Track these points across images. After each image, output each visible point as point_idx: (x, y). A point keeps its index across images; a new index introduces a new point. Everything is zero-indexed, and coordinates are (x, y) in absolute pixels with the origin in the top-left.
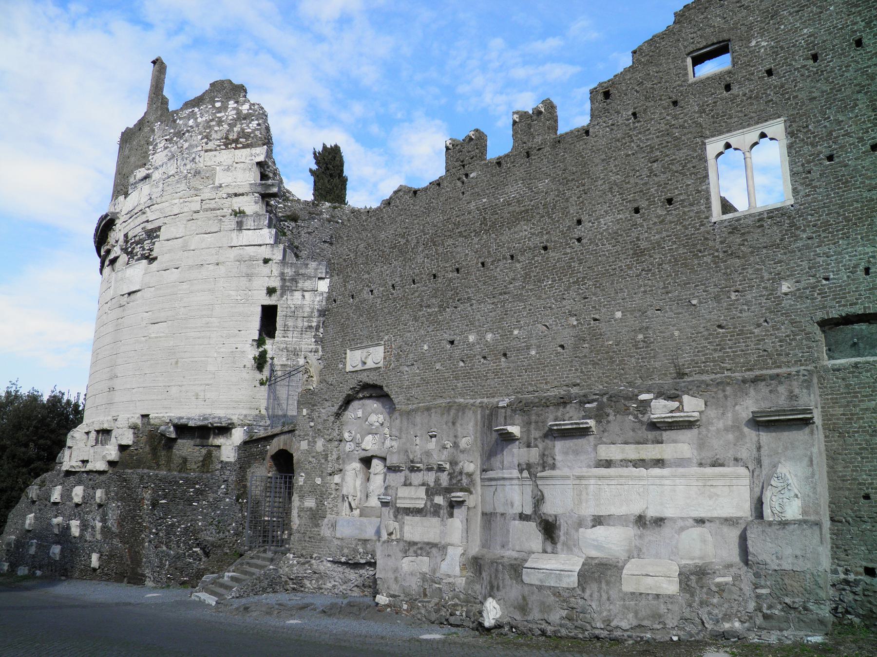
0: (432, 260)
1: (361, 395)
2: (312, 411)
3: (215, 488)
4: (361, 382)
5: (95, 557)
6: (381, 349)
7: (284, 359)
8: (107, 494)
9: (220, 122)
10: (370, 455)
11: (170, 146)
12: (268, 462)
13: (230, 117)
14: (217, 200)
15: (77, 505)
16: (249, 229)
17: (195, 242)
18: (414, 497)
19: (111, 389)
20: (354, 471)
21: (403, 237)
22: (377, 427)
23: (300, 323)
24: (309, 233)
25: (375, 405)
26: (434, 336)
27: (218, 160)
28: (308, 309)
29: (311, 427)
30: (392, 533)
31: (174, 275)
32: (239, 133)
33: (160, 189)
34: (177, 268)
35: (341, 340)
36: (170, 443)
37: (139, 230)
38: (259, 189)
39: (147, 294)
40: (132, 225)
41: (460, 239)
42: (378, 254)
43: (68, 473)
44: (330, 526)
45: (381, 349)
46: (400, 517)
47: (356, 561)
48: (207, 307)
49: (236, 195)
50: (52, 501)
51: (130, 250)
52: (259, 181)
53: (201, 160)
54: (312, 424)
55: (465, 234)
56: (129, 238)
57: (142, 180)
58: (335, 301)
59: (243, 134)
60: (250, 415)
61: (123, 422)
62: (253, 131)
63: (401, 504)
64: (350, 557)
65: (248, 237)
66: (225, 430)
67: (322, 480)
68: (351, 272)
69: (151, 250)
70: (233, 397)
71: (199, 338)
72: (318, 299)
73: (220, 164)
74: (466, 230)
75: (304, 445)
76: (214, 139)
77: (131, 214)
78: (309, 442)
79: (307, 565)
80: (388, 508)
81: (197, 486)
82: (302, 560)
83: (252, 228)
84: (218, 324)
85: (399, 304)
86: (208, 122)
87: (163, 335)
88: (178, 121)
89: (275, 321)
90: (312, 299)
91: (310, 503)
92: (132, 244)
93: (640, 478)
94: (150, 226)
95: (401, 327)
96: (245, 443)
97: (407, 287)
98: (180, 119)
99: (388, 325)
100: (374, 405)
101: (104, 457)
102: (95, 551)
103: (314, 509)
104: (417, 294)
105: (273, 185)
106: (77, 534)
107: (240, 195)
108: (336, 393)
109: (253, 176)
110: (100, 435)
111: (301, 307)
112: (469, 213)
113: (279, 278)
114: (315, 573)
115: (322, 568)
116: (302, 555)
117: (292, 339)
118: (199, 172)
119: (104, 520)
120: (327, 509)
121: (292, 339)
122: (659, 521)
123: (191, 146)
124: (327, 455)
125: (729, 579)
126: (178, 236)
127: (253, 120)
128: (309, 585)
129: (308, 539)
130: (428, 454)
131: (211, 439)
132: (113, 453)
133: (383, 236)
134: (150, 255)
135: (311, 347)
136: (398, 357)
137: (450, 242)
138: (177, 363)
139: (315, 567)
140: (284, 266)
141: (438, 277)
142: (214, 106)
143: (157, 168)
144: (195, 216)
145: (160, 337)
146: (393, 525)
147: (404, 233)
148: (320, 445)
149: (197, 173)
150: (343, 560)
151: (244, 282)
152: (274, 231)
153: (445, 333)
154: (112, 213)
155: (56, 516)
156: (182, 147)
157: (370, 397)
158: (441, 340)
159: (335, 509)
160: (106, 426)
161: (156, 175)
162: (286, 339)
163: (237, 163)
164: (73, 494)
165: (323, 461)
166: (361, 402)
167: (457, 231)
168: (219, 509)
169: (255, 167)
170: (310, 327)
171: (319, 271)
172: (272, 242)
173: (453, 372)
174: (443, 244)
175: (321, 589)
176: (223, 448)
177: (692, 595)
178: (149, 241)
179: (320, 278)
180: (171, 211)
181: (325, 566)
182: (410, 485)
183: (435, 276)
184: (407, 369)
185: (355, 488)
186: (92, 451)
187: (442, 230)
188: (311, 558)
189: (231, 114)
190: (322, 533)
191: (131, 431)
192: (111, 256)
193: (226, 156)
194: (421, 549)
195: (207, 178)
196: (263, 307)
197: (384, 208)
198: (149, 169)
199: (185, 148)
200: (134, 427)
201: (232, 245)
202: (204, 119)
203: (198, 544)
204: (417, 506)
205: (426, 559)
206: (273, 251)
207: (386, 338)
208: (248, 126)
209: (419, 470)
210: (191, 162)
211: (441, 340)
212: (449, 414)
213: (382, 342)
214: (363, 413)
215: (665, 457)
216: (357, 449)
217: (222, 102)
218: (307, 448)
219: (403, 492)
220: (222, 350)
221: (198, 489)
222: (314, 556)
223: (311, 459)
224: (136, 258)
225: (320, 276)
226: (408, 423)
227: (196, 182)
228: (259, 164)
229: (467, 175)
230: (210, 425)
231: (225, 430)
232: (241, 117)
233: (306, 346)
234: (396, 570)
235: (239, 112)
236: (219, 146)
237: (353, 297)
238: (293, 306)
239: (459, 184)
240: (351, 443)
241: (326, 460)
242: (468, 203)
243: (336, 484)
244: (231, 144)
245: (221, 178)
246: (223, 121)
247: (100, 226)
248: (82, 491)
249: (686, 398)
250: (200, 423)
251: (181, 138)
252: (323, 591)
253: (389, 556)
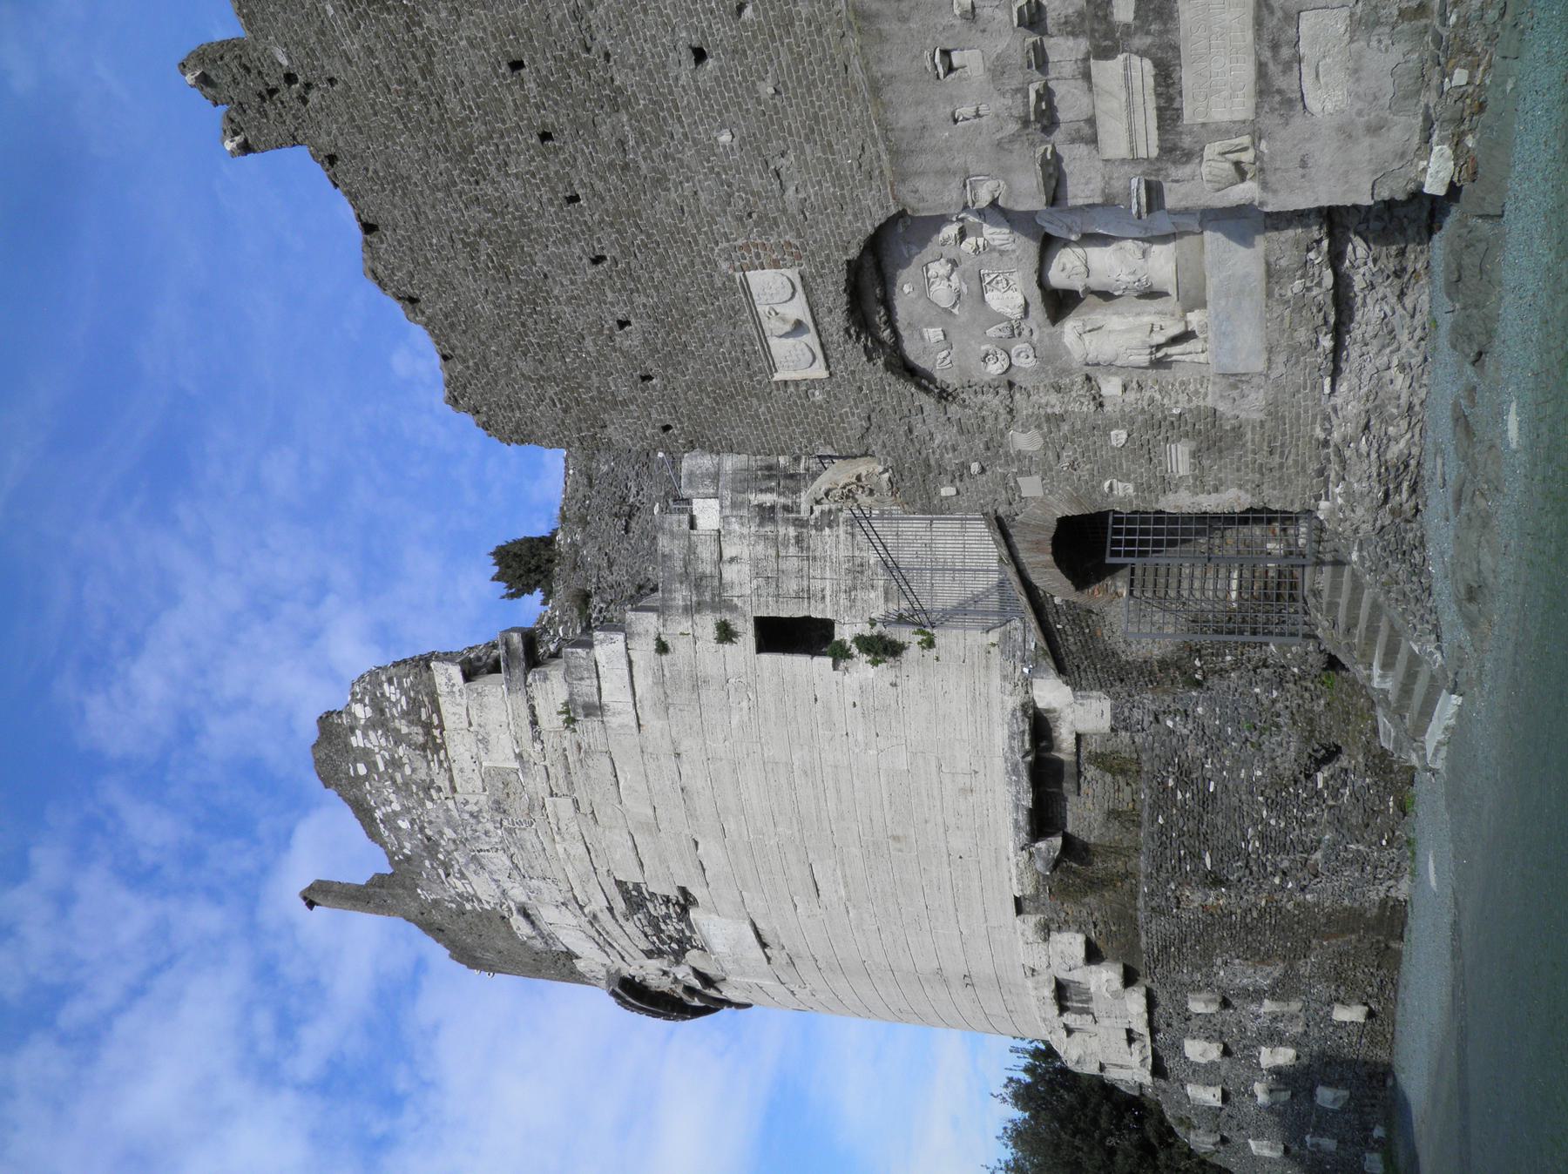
0: (508, 151)
1: (886, 334)
2: (942, 470)
3: (1175, 741)
4: (847, 331)
5: (1342, 1014)
6: (756, 278)
7: (873, 595)
8: (1200, 989)
9: (395, 763)
10: (1037, 292)
11: (456, 867)
12: (1094, 597)
13: (383, 741)
14: (547, 763)
15: (1226, 1052)
16: (599, 689)
17: (639, 809)
18: (1123, 96)
19: (968, 980)
20: (1086, 337)
21: (473, 248)
22: (963, 278)
23: (792, 564)
24: (611, 564)
25: (906, 289)
26: (692, 114)
27: (468, 764)
28: (760, 548)
29: (983, 470)
30: (1237, 164)
31: (711, 851)
32: (411, 723)
33: (542, 884)
34: (696, 843)
35: (755, 401)
36: (1073, 849)
37: (630, 927)
39: (757, 907)
40: (624, 942)
41: (439, 70)
42: (530, 316)
43: (1158, 1070)
44: (1235, 393)
45: (756, 278)
46: (1187, 142)
47: (1329, 301)
48: (770, 775)
50: (1219, 1104)
51: (674, 946)
52: (502, 676)
53: (472, 799)
54: (975, 467)
55: (421, 53)
56: (651, 947)
57: (533, 923)
58: (666, 428)
59: (411, 714)
60: (1003, 668)
61: (1035, 955)
62: (404, 692)
63: (1149, 146)
64: (1320, 321)
65: (614, 691)
66: (1039, 726)
67: (1116, 426)
68: (589, 389)
69: (667, 900)
70: (964, 708)
71: (838, 791)
72: (736, 527)
73: (476, 760)
74: (414, 57)
75: (1031, 486)
76: (428, 774)
77: (605, 944)
78: (1021, 473)
79: (1348, 453)
80: (1166, 186)
81: (1171, 783)
82: (1333, 469)
83: (595, 682)
84: (806, 748)
85: (635, 236)
86: (397, 787)
87: (839, 872)
88: (406, 851)
89: (791, 619)
90: (736, 540)
91: (1179, 458)
92: (663, 943)
94: (620, 905)
95: (689, 223)
96: (1061, 670)
97: (587, 218)
98: (401, 847)
99: (692, 263)
100: (905, 289)
101: (1115, 995)
102: (1329, 1014)
103: (1193, 444)
104: (599, 186)
107: (533, 714)
108: (889, 403)
109: (493, 688)
110: (1069, 1004)
111: (756, 563)
112: (370, 52)
113: (697, 617)
114: (1367, 427)
115: (1353, 409)
116: (1321, 472)
117: (826, 580)
118: (497, 802)
119: (1257, 995)
120: (1193, 405)
121: (826, 580)
123: (449, 822)
124: (1048, 418)
126: (630, 844)
127: (383, 694)
128: (1402, 443)
129: (1277, 459)
130: (998, 70)
131: (1062, 756)
132: (1104, 978)
133: (485, 308)
134: (678, 903)
135: (842, 536)
136: (767, 223)
137: (452, 102)
138: (896, 838)
139: (1350, 429)
140: (669, 608)
141: (544, 124)
142: (367, 777)
143: (504, 892)
144: (584, 808)
145: (844, 876)
146: (1213, 162)
147: (465, 245)
148: (1024, 441)
149: (498, 807)
150: (1327, 342)
151: (710, 695)
153: (677, 79)
155: (1253, 1096)
156: (454, 841)
157: (887, 303)
158: (698, 89)
159: (1192, 388)
160: (1048, 992)
161: (518, 894)
162: (828, 593)
163: (470, 724)
164: (1203, 1061)
165: (1065, 427)
166: (904, 333)
167: (422, 83)
168: (1221, 730)
169: (473, 685)
170: (799, 540)
171: (675, 528)
172: (620, 637)
173: (772, 36)
174: (462, 123)
175: (1410, 407)
176: (1081, 728)
178: (650, 905)
179: (693, 525)
180: (582, 860)
181: (1349, 399)
182: (1091, 121)
183: (545, 136)
184: (791, 191)
185: (1128, 331)
186: (1105, 1022)
187: (430, 131)
188: (1326, 443)
189: (376, 740)
190: (1257, 416)
191: (1055, 936)
192: (697, 984)
193: (460, 748)
194: (1275, 47)
195: (506, 785)
196: (761, 649)
197: (423, 313)
198: (510, 909)
199: (454, 836)
200: (1046, 930)
201: (634, 724)
202: (393, 797)
203: (1308, 777)
204: (1150, 82)
205: (1307, 22)
206: (639, 634)
207: (724, 266)
208: (395, 704)
209: (1046, 95)
210: (479, 822)
211: (698, 89)
212: (877, 15)
213: (738, 275)
214: (931, 325)
216: (1026, 333)
217: (356, 761)
218: (1037, 478)
219: (1114, 142)
220: (860, 738)
221: (1177, 780)
222: (1322, 436)
223: (1065, 463)
224: (688, 933)
225: (686, 526)
226: (923, 151)
227: (518, 807)
229: (290, 78)
230: (1029, 759)
231: (1039, 726)
232: (380, 721)
233: (841, 546)
234: (1346, 133)
235: (372, 725)
236: (440, 763)
237: (646, 378)
238: (754, 585)
239: (314, 97)
240: (1013, 353)
241: (1061, 418)
242: (350, 62)
243: (1125, 388)
244: (434, 738)
245: (502, 756)
246: (392, 757)
247: (642, 1009)
248: (1196, 1042)
250: (1025, 782)
251: (438, 845)
252: (1416, 401)
253: (1303, 164)
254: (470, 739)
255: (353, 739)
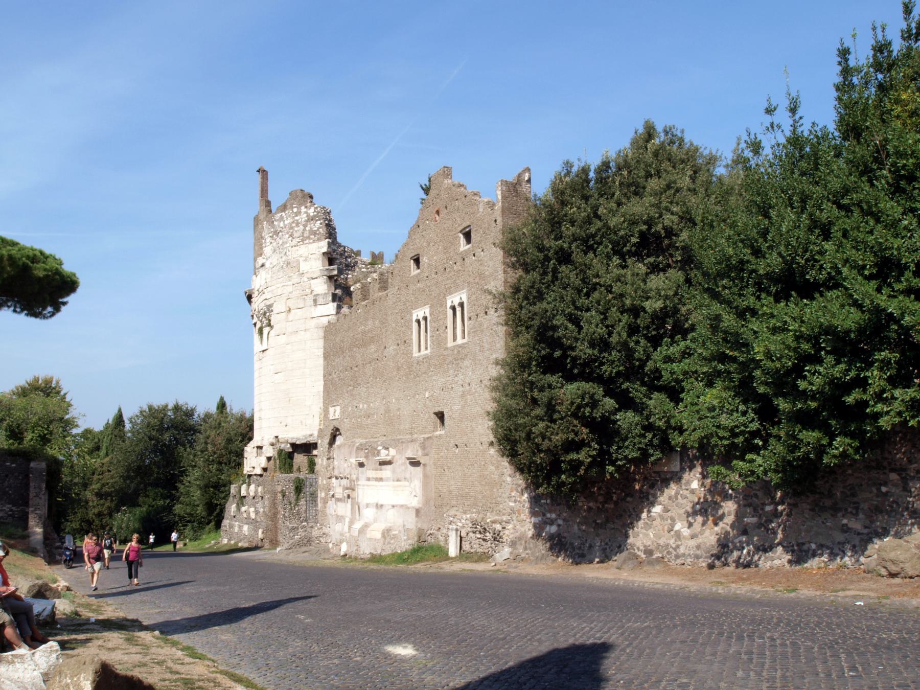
9: (298, 224)
31: (283, 339)
36: (290, 456)
38: (326, 273)
49: (313, 279)
62: (319, 228)
93: (376, 486)
94: (268, 303)
98: (276, 220)
105: (333, 269)
106: (254, 517)
122: (382, 506)
123: (284, 243)
125: (397, 532)
127: (317, 220)
149: (289, 263)
152: (335, 304)
154: (249, 290)
177: (385, 539)
193: (303, 250)
215: (384, 477)
228: (324, 253)
232: (311, 219)
235: (308, 215)
245: (304, 267)
249: (390, 449)
254: (306, 254)
255: (303, 208)
